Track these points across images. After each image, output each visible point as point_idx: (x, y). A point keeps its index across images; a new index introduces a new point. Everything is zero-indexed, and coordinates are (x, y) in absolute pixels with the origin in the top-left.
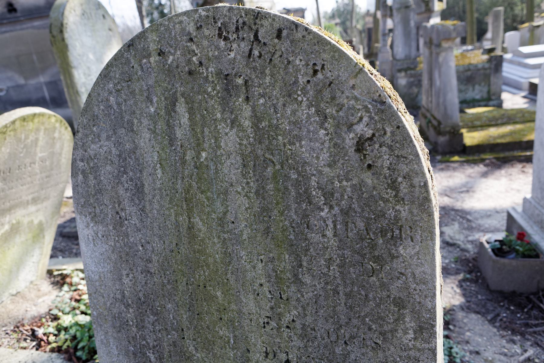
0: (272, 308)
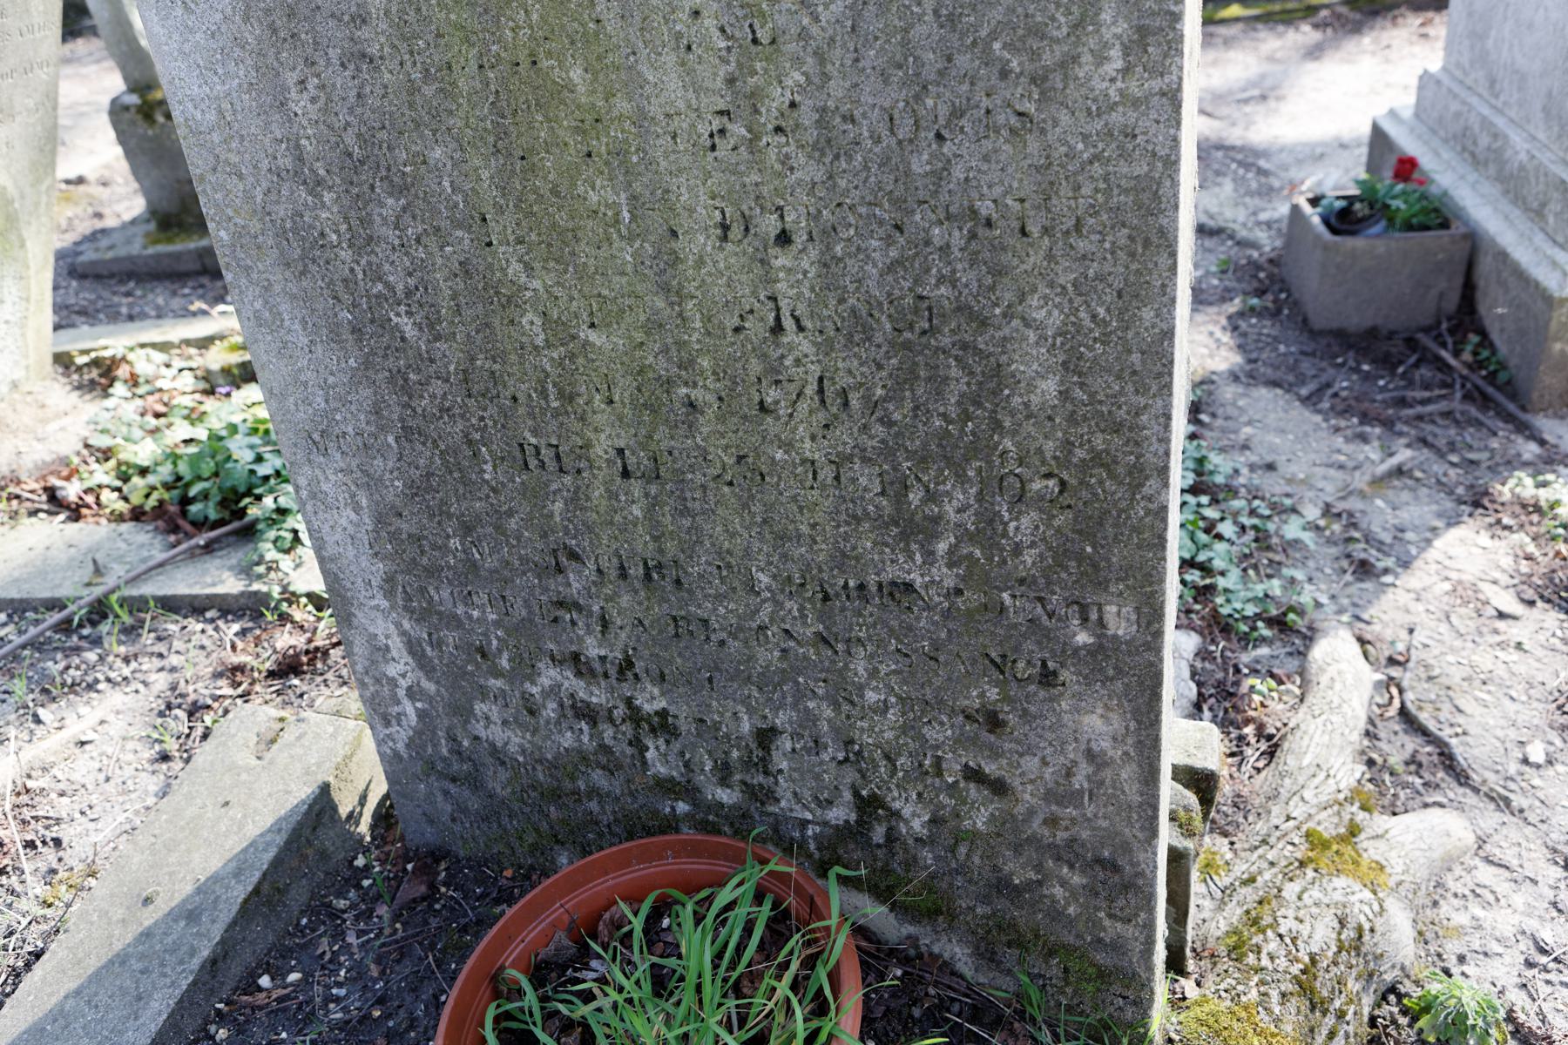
0: (731, 81)
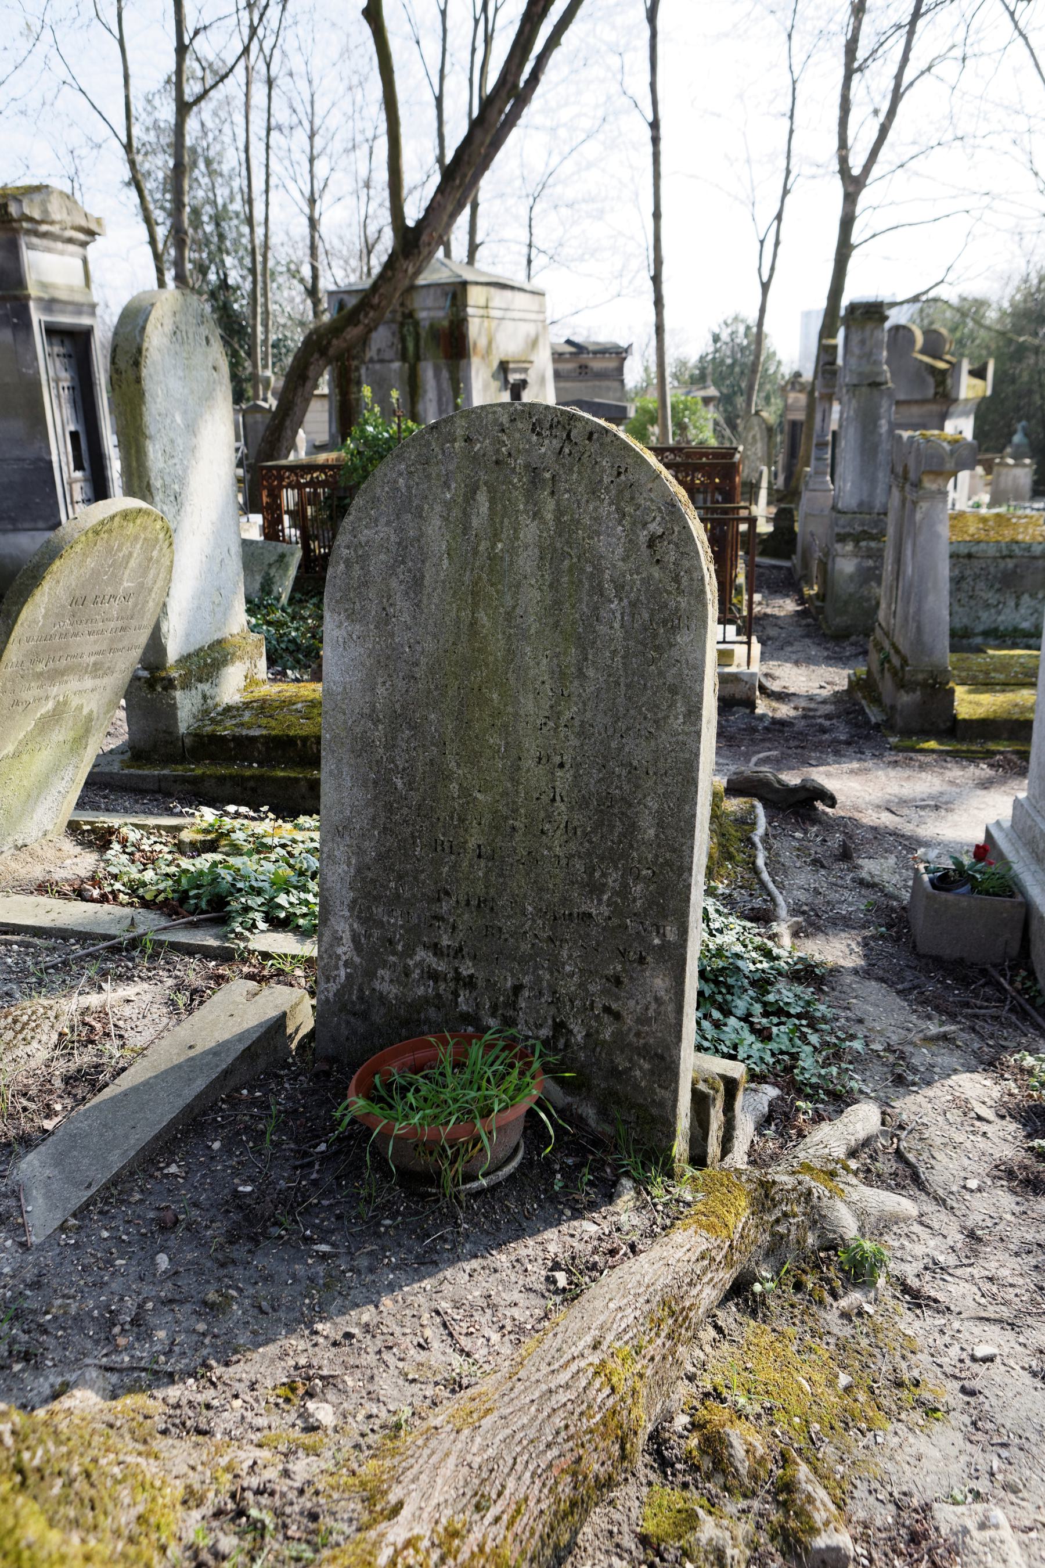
0: (551, 707)
